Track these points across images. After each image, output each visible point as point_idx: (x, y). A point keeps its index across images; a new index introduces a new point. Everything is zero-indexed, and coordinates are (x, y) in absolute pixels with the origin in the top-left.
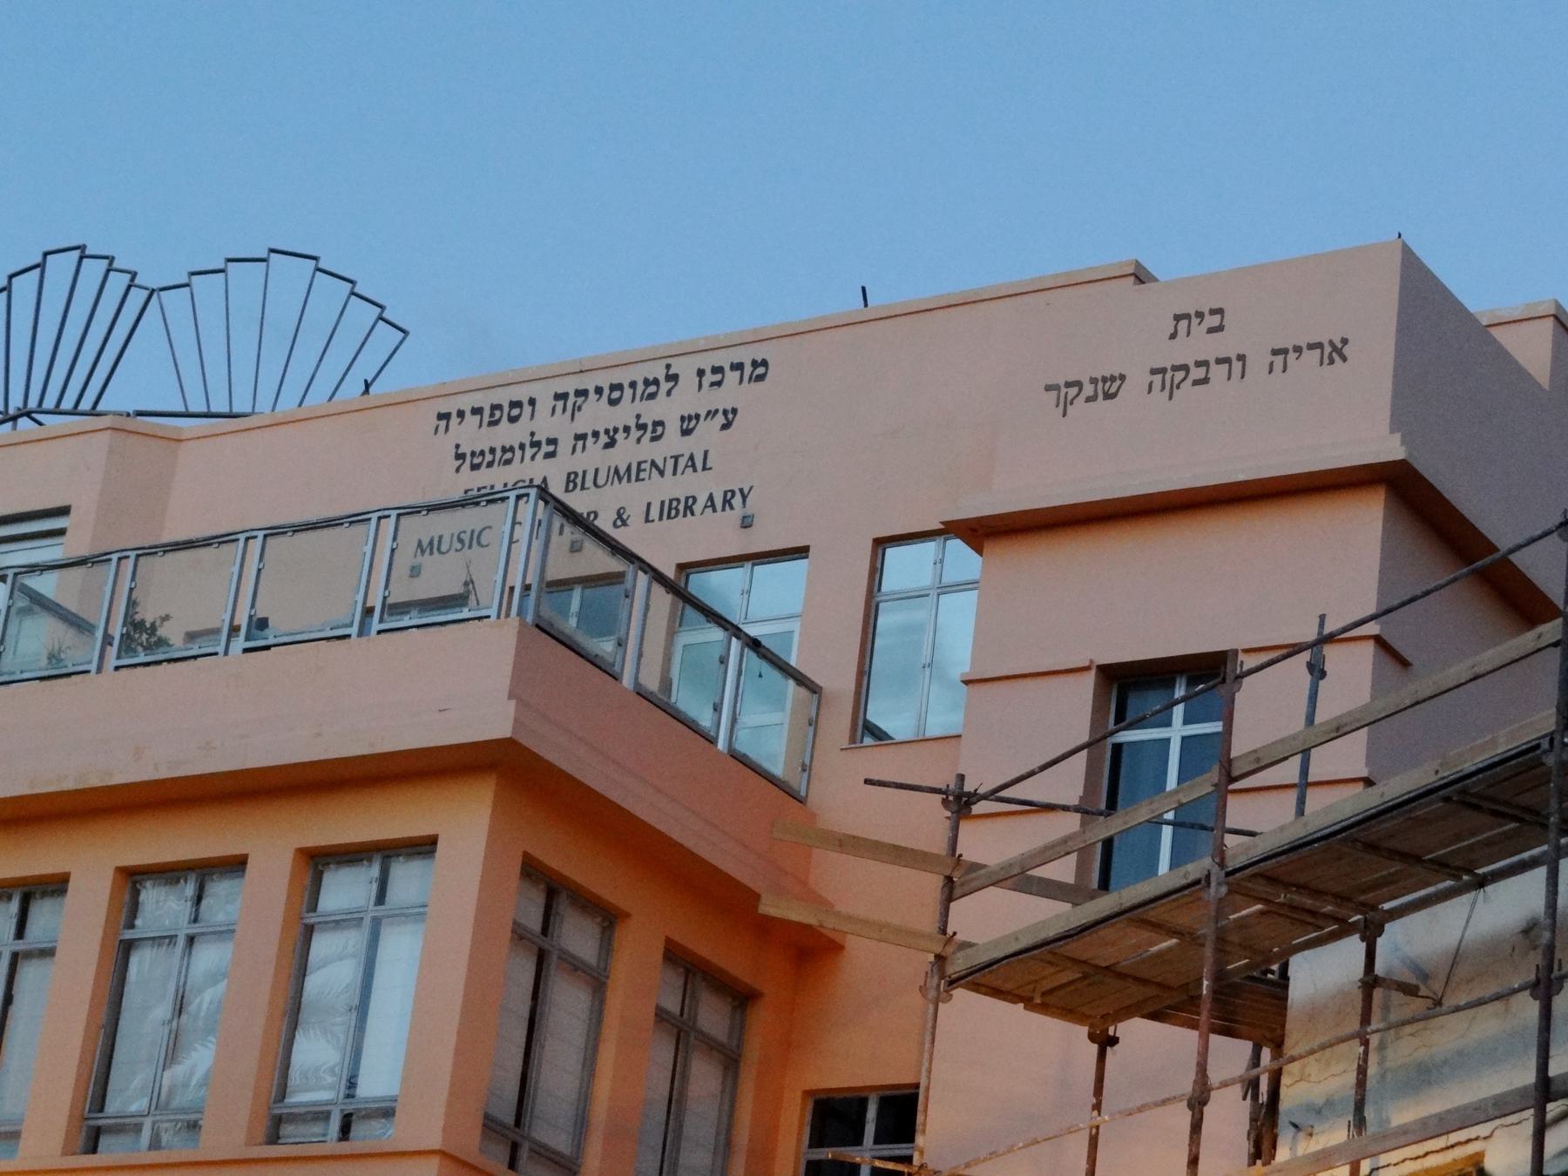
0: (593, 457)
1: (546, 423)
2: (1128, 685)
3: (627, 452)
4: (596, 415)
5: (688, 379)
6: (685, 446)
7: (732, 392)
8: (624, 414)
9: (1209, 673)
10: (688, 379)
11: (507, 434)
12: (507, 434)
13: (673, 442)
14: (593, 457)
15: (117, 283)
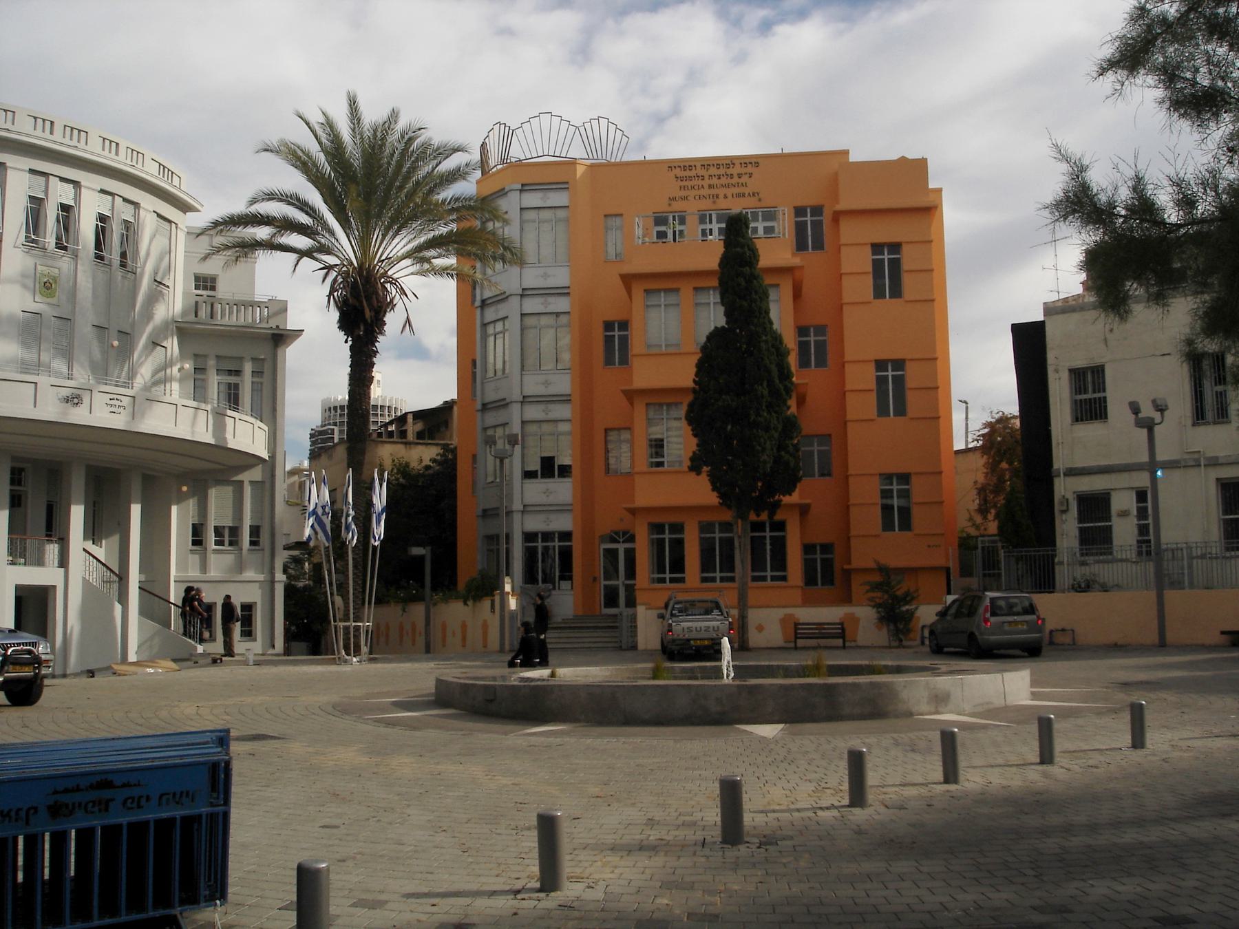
0: (715, 181)
1: (701, 172)
2: (877, 248)
3: (724, 181)
4: (713, 171)
5: (738, 165)
6: (741, 181)
7: (750, 169)
8: (722, 171)
9: (895, 247)
10: (738, 165)
11: (688, 173)
12: (688, 173)
13: (735, 180)
14: (715, 181)
15: (565, 124)
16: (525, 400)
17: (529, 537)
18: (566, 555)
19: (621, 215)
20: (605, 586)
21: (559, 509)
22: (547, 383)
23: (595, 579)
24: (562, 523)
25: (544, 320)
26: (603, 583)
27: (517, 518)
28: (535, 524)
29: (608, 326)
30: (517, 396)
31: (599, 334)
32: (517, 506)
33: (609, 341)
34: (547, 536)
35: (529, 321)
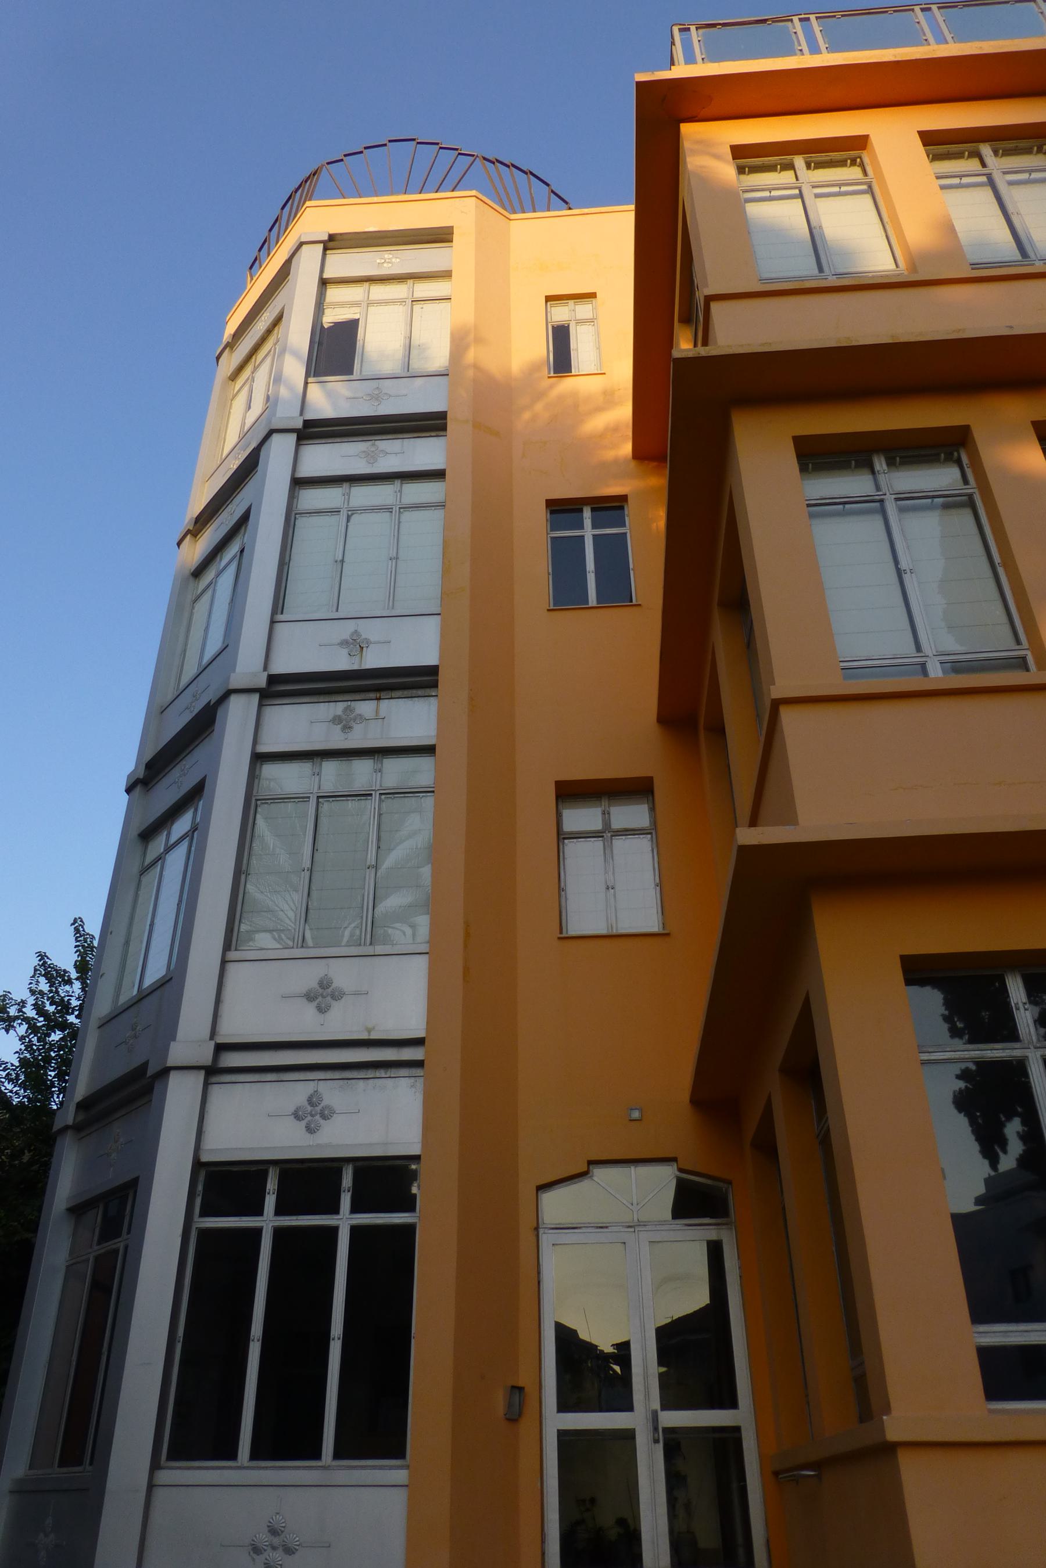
16: (280, 688)
17: (226, 1184)
18: (386, 1260)
19: (592, 295)
20: (564, 1436)
21: (375, 1058)
22: (357, 645)
23: (518, 1401)
24: (383, 1120)
25: (363, 495)
26: (556, 1421)
27: (180, 1095)
28: (256, 1124)
29: (563, 509)
30: (248, 668)
31: (533, 532)
32: (189, 1043)
33: (565, 558)
34: (309, 1182)
35: (311, 498)
